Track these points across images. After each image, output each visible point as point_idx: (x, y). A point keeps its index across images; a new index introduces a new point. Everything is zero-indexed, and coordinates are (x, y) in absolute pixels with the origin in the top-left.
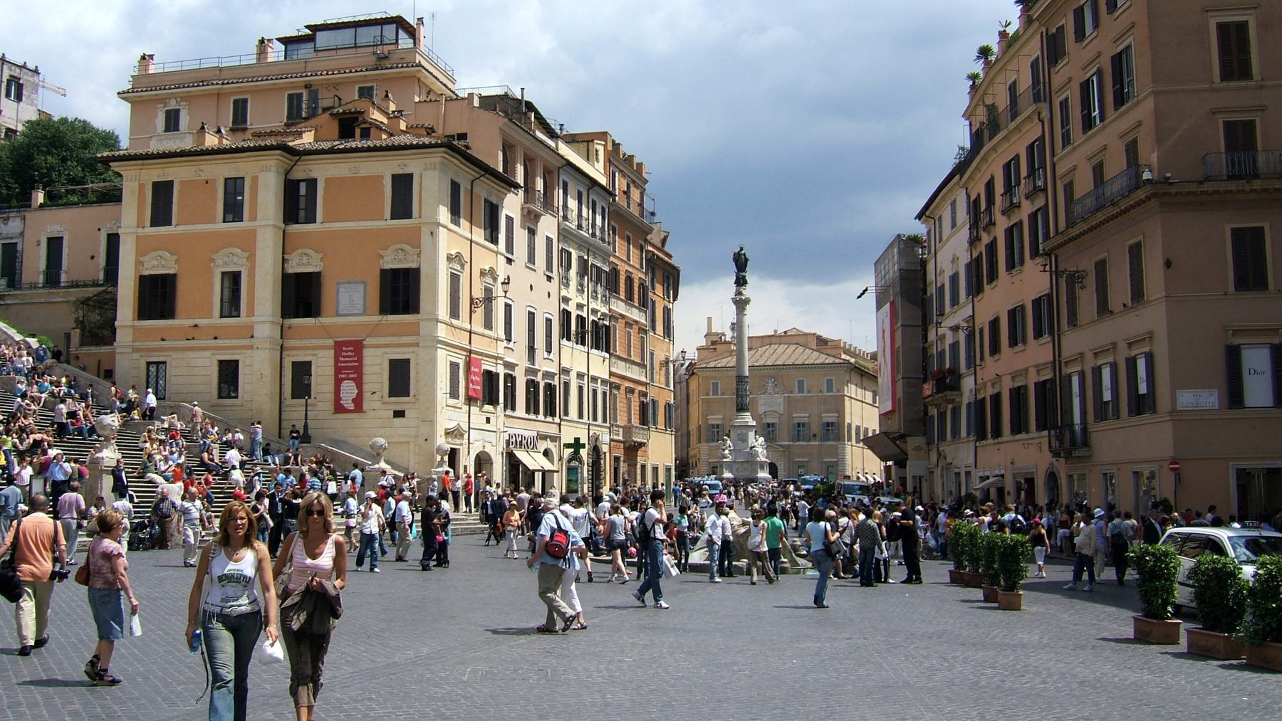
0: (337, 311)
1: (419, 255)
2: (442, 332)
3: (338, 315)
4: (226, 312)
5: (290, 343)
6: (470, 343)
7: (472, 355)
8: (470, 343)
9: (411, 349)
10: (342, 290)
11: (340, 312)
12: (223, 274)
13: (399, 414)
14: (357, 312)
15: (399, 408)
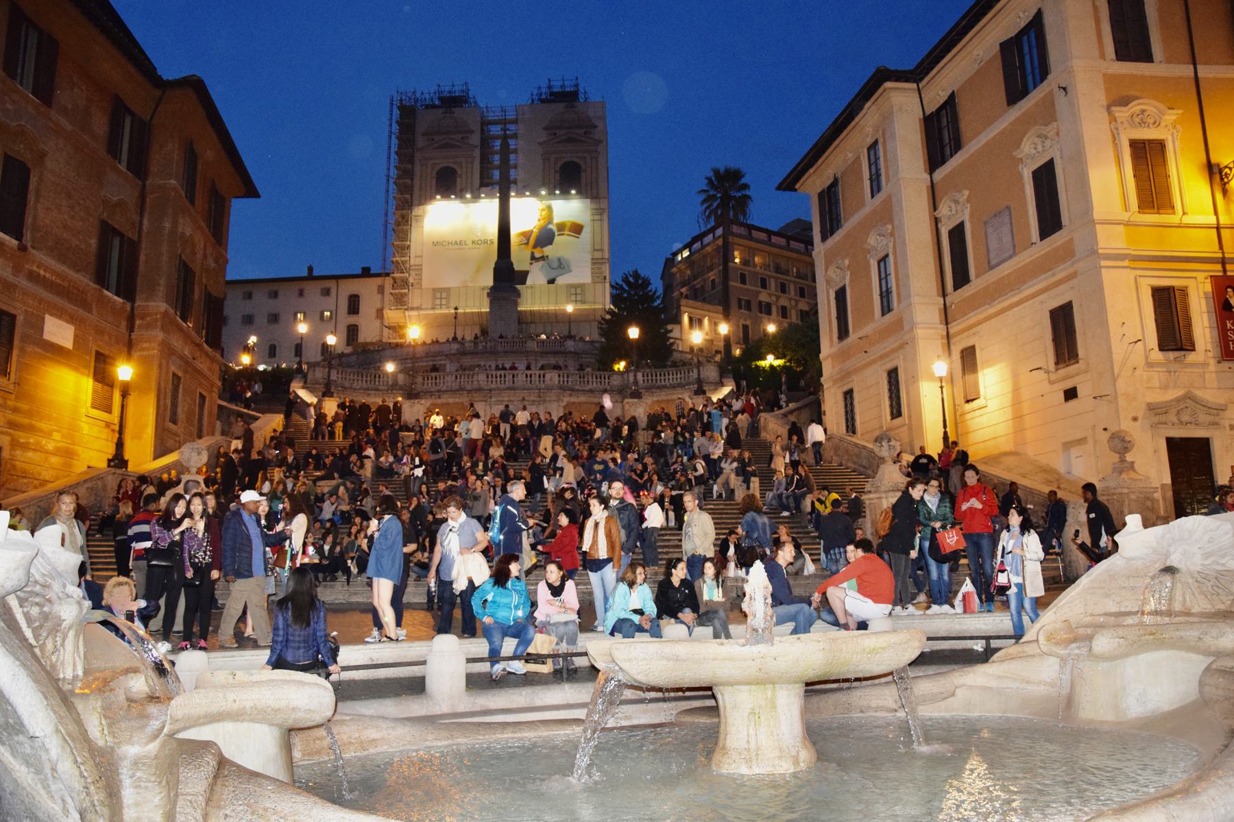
0: (989, 262)
1: (1058, 134)
2: (1110, 239)
3: (991, 268)
4: (886, 309)
5: (954, 328)
6: (1221, 247)
7: (1228, 267)
8: (1221, 247)
9: (1071, 283)
10: (990, 230)
11: (993, 263)
12: (879, 263)
13: (1071, 394)
14: (1006, 255)
15: (1068, 385)
